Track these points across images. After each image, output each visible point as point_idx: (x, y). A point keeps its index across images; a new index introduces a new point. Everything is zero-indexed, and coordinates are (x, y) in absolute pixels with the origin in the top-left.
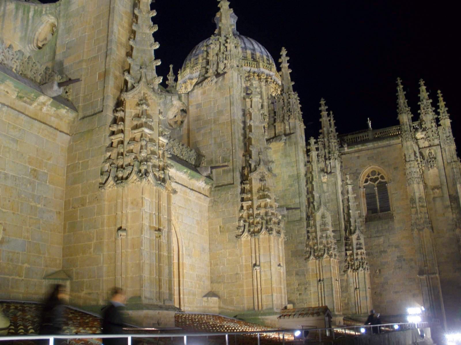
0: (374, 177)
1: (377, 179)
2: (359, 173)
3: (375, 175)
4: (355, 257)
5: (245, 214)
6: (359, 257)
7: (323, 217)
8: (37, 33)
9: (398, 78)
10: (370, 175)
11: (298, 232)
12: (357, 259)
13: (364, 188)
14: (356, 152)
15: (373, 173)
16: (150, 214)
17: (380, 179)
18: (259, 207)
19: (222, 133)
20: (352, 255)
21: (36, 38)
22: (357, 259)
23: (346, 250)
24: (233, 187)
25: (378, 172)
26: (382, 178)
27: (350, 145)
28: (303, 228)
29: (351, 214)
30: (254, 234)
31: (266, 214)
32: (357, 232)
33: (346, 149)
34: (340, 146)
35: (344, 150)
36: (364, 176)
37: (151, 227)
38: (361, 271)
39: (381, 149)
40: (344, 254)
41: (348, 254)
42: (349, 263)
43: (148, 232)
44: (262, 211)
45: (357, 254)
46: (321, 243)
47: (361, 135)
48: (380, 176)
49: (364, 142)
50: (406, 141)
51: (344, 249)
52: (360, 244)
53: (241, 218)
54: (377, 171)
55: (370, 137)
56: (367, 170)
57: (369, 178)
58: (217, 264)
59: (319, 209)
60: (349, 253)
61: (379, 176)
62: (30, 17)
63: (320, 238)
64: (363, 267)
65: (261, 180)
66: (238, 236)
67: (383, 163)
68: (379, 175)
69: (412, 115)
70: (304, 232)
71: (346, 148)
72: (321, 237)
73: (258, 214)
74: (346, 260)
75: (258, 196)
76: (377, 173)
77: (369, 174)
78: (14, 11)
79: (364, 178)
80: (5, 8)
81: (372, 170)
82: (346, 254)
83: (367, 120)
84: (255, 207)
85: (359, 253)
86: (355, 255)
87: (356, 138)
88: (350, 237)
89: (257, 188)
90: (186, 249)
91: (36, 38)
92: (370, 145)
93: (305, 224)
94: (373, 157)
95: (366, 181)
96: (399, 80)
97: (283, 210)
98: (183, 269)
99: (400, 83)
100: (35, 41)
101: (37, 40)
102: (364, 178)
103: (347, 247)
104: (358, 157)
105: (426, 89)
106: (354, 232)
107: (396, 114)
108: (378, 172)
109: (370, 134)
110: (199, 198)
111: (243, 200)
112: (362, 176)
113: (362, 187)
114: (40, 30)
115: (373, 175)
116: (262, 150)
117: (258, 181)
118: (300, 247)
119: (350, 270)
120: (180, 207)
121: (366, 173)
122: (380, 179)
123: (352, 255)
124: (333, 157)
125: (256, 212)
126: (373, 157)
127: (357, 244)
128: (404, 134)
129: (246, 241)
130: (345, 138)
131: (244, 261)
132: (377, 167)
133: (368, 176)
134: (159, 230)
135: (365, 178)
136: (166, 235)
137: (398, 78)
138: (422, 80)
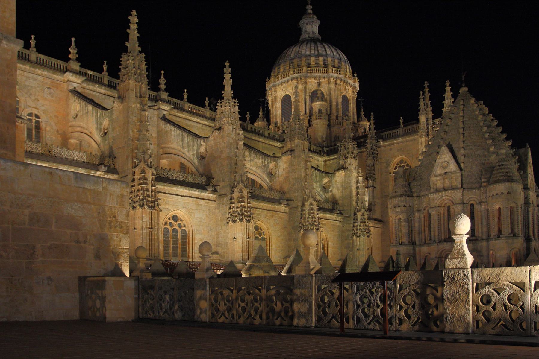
0: (401, 165)
1: (403, 166)
2: (390, 162)
3: (403, 163)
4: (359, 228)
5: (231, 211)
6: (362, 228)
7: (311, 204)
8: (103, 126)
9: (426, 82)
10: (399, 163)
11: (296, 214)
12: (360, 229)
13: (394, 173)
14: (389, 145)
15: (401, 161)
16: (146, 222)
17: (406, 167)
18: (237, 207)
19: (223, 164)
20: (357, 226)
21: (103, 128)
22: (360, 229)
23: (354, 223)
24: (226, 196)
25: (405, 161)
26: (408, 165)
27: (384, 139)
28: (298, 212)
29: (360, 198)
30: (234, 221)
31: (241, 210)
32: (363, 210)
33: (382, 143)
34: (376, 141)
35: (381, 144)
36: (394, 164)
37: (146, 227)
38: (362, 238)
39: (408, 143)
40: (352, 225)
41: (355, 226)
42: (355, 232)
43: (145, 230)
44: (239, 210)
45: (360, 226)
46: (308, 221)
47: (394, 131)
48: (406, 163)
49: (396, 136)
50: (421, 139)
51: (352, 222)
52: (364, 219)
53: (230, 213)
54: (404, 160)
55: (401, 133)
56: (397, 159)
57: (398, 166)
58: (219, 237)
59: (307, 201)
60: (355, 225)
61: (406, 164)
62: (99, 117)
63: (307, 219)
64: (363, 235)
65: (239, 193)
66: (228, 223)
67: (408, 154)
68: (405, 163)
69: (433, 115)
70: (299, 214)
71: (382, 143)
72: (308, 218)
73: (237, 211)
74: (353, 230)
75: (237, 201)
76: (404, 162)
77: (398, 162)
78: (92, 110)
79: (394, 166)
80: (88, 108)
81: (400, 160)
82: (354, 226)
83: (400, 119)
84: (235, 207)
85: (362, 225)
86: (359, 226)
87: (396, 132)
88: (357, 214)
89: (237, 196)
90: (197, 231)
91: (103, 128)
92: (400, 140)
93: (300, 209)
94: (401, 149)
95: (396, 168)
96: (426, 84)
97: (284, 201)
98: (195, 241)
99: (426, 87)
100: (103, 130)
101: (104, 129)
102: (394, 166)
103: (355, 221)
104: (391, 149)
105: (451, 89)
106: (360, 211)
107: (418, 115)
108: (405, 161)
109: (401, 130)
110: (207, 203)
111: (231, 203)
112: (393, 164)
113: (392, 173)
114: (104, 124)
115: (401, 163)
116: (242, 175)
117: (238, 192)
118: (296, 224)
119: (355, 237)
120: (192, 209)
121: (396, 162)
122: (406, 167)
123: (357, 226)
124: (349, 157)
125: (235, 210)
126: (401, 149)
127: (361, 219)
128: (420, 132)
129: (232, 225)
130: (383, 134)
131: (230, 236)
132: (404, 157)
133: (398, 164)
134: (152, 228)
135: (395, 165)
136: (157, 229)
137: (426, 82)
138: (448, 81)
